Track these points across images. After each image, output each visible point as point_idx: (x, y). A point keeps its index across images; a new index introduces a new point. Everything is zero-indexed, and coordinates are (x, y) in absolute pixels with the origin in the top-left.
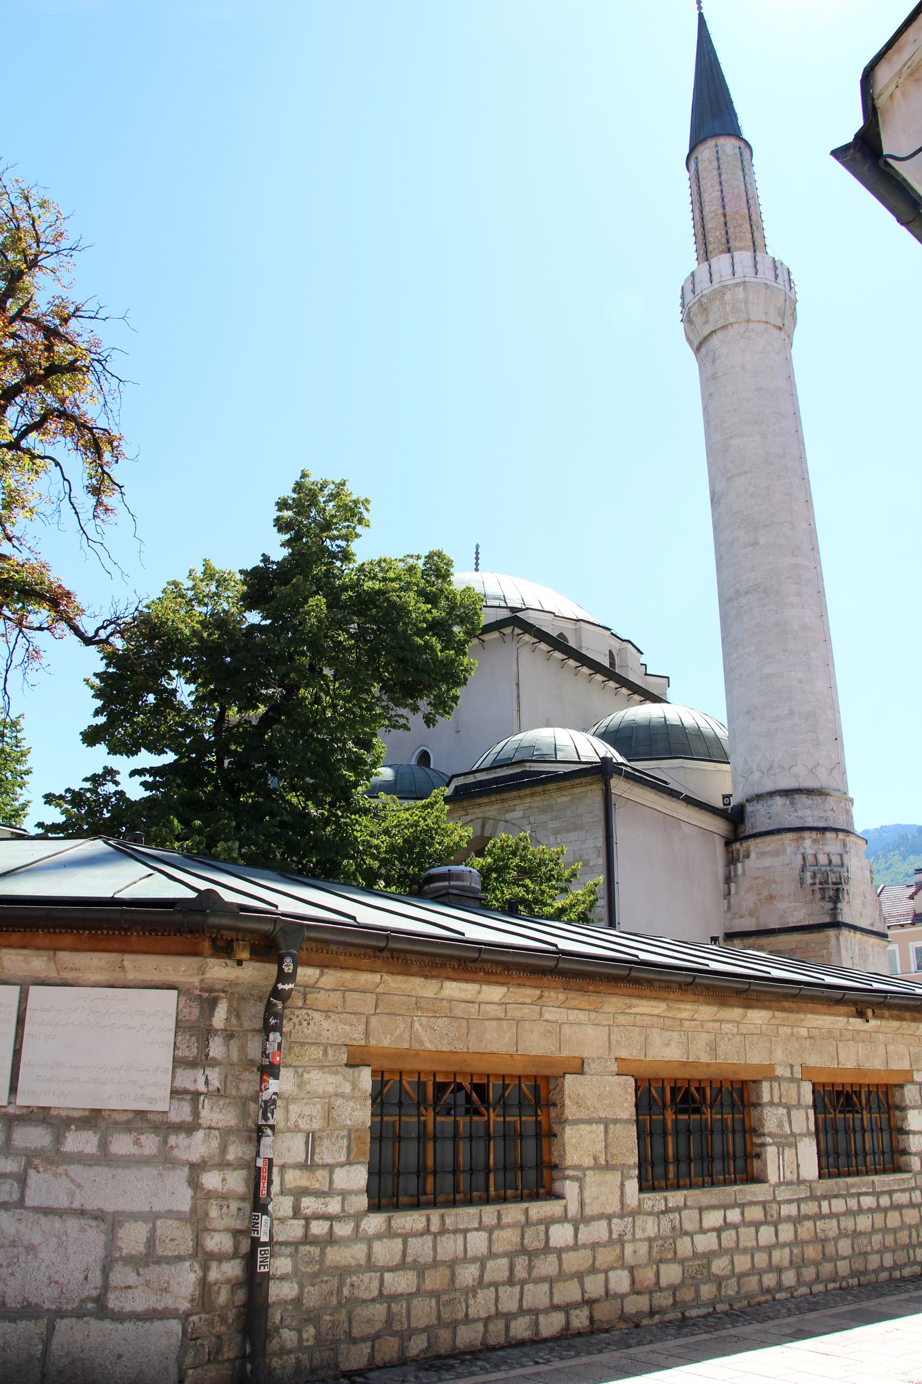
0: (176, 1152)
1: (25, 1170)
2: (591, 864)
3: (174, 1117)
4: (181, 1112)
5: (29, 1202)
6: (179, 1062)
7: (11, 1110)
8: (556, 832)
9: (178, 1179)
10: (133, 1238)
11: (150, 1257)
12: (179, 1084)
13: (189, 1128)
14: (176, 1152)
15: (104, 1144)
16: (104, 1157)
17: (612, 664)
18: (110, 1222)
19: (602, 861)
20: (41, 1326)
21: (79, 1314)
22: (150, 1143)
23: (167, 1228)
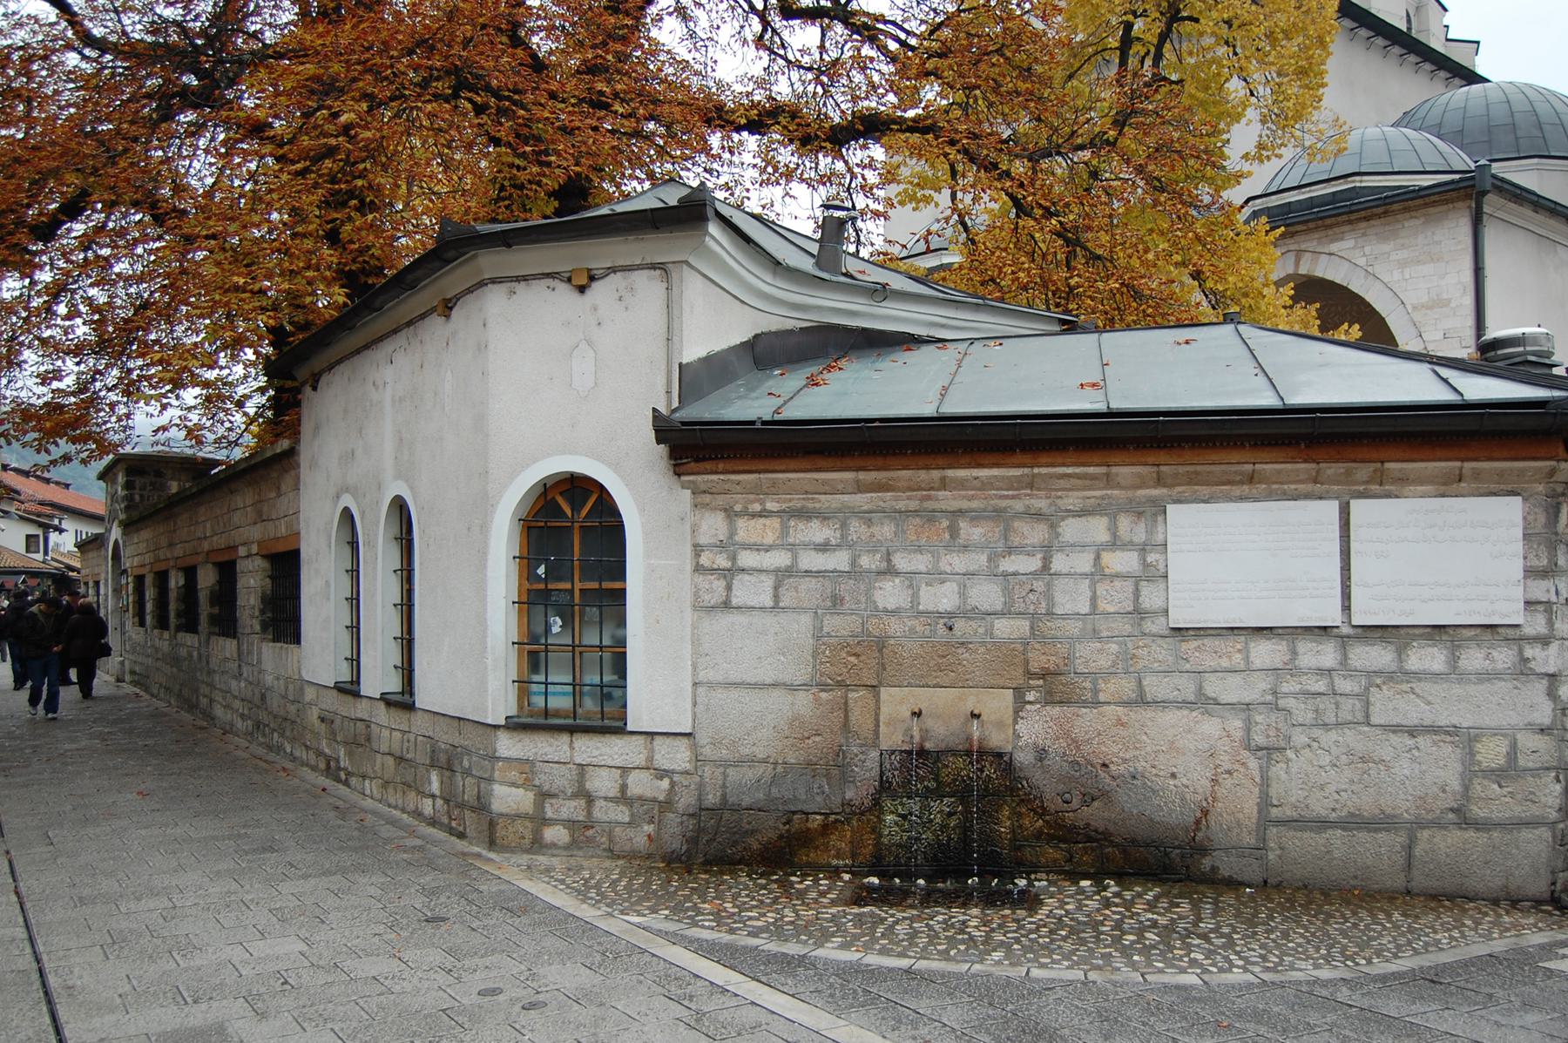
0: (1532, 665)
1: (1367, 689)
2: (1453, 305)
3: (1528, 631)
4: (1537, 625)
5: (1375, 720)
6: (1531, 573)
7: (1346, 630)
8: (1403, 264)
9: (1537, 691)
10: (1492, 753)
11: (1508, 772)
12: (1533, 597)
13: (1544, 641)
14: (1532, 665)
15: (1453, 661)
16: (1454, 671)
17: (1409, 29)
18: (1466, 739)
19: (1469, 300)
20: (1401, 839)
21: (1437, 824)
22: (1504, 657)
23: (1528, 741)
